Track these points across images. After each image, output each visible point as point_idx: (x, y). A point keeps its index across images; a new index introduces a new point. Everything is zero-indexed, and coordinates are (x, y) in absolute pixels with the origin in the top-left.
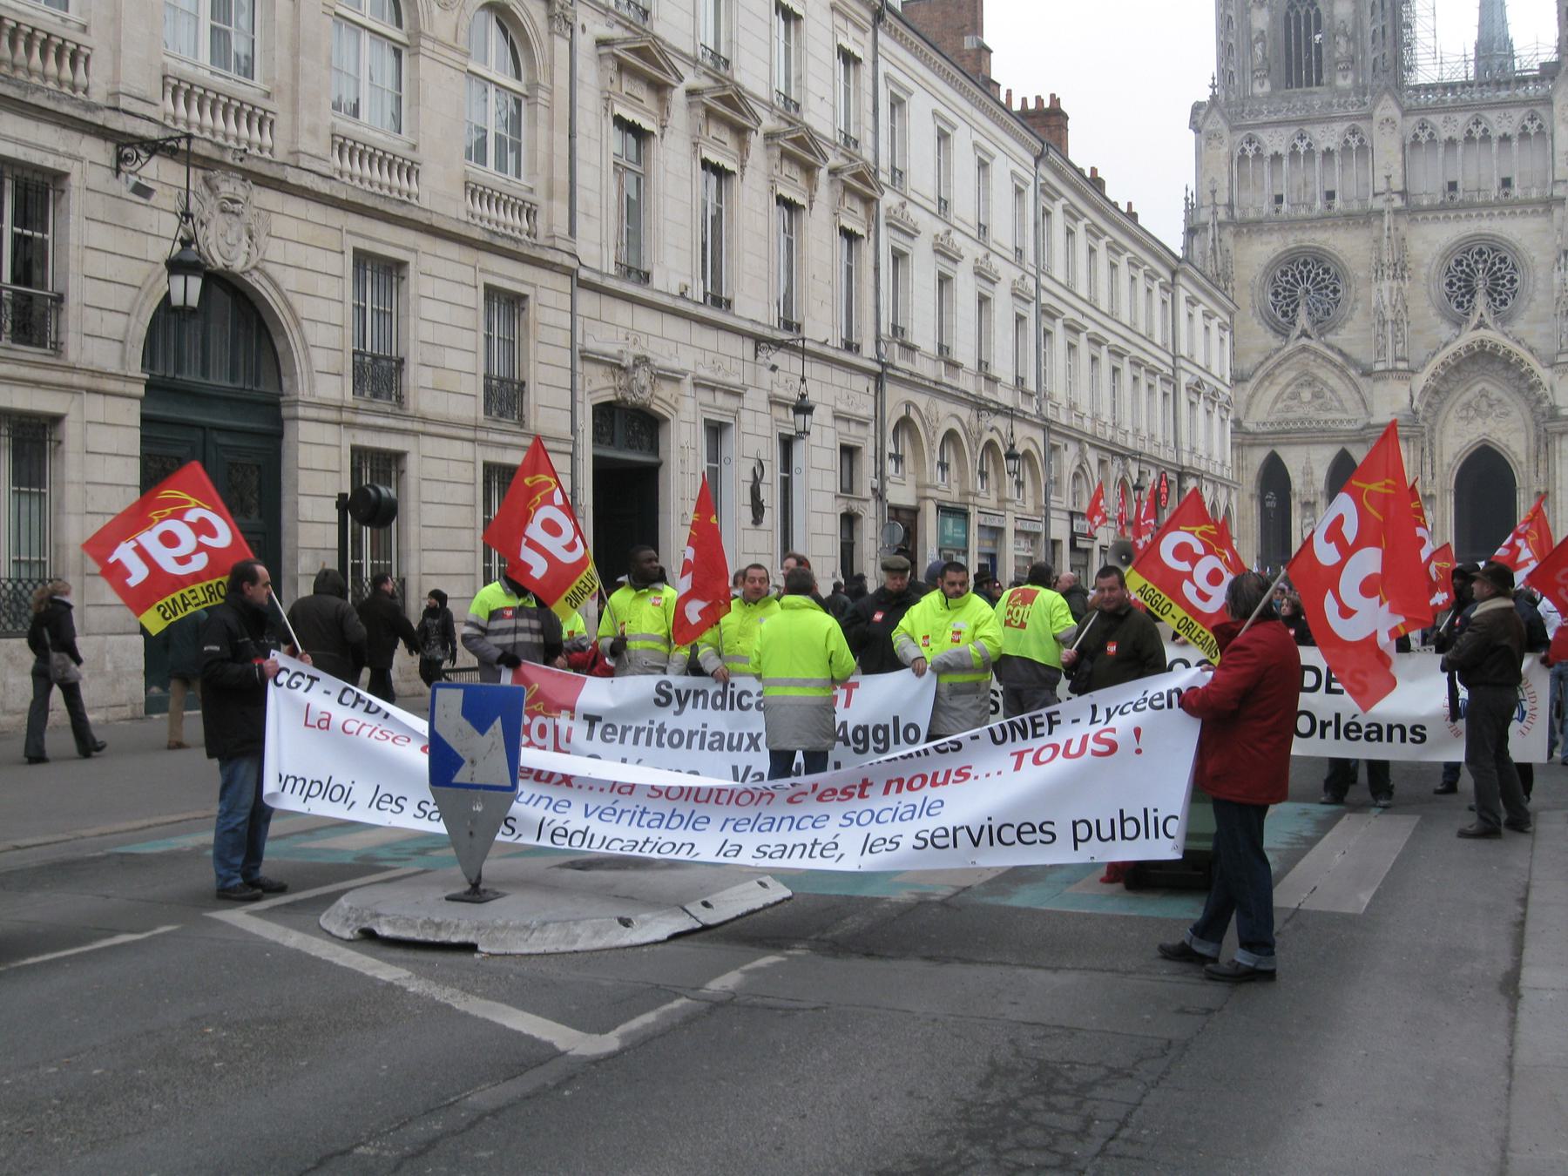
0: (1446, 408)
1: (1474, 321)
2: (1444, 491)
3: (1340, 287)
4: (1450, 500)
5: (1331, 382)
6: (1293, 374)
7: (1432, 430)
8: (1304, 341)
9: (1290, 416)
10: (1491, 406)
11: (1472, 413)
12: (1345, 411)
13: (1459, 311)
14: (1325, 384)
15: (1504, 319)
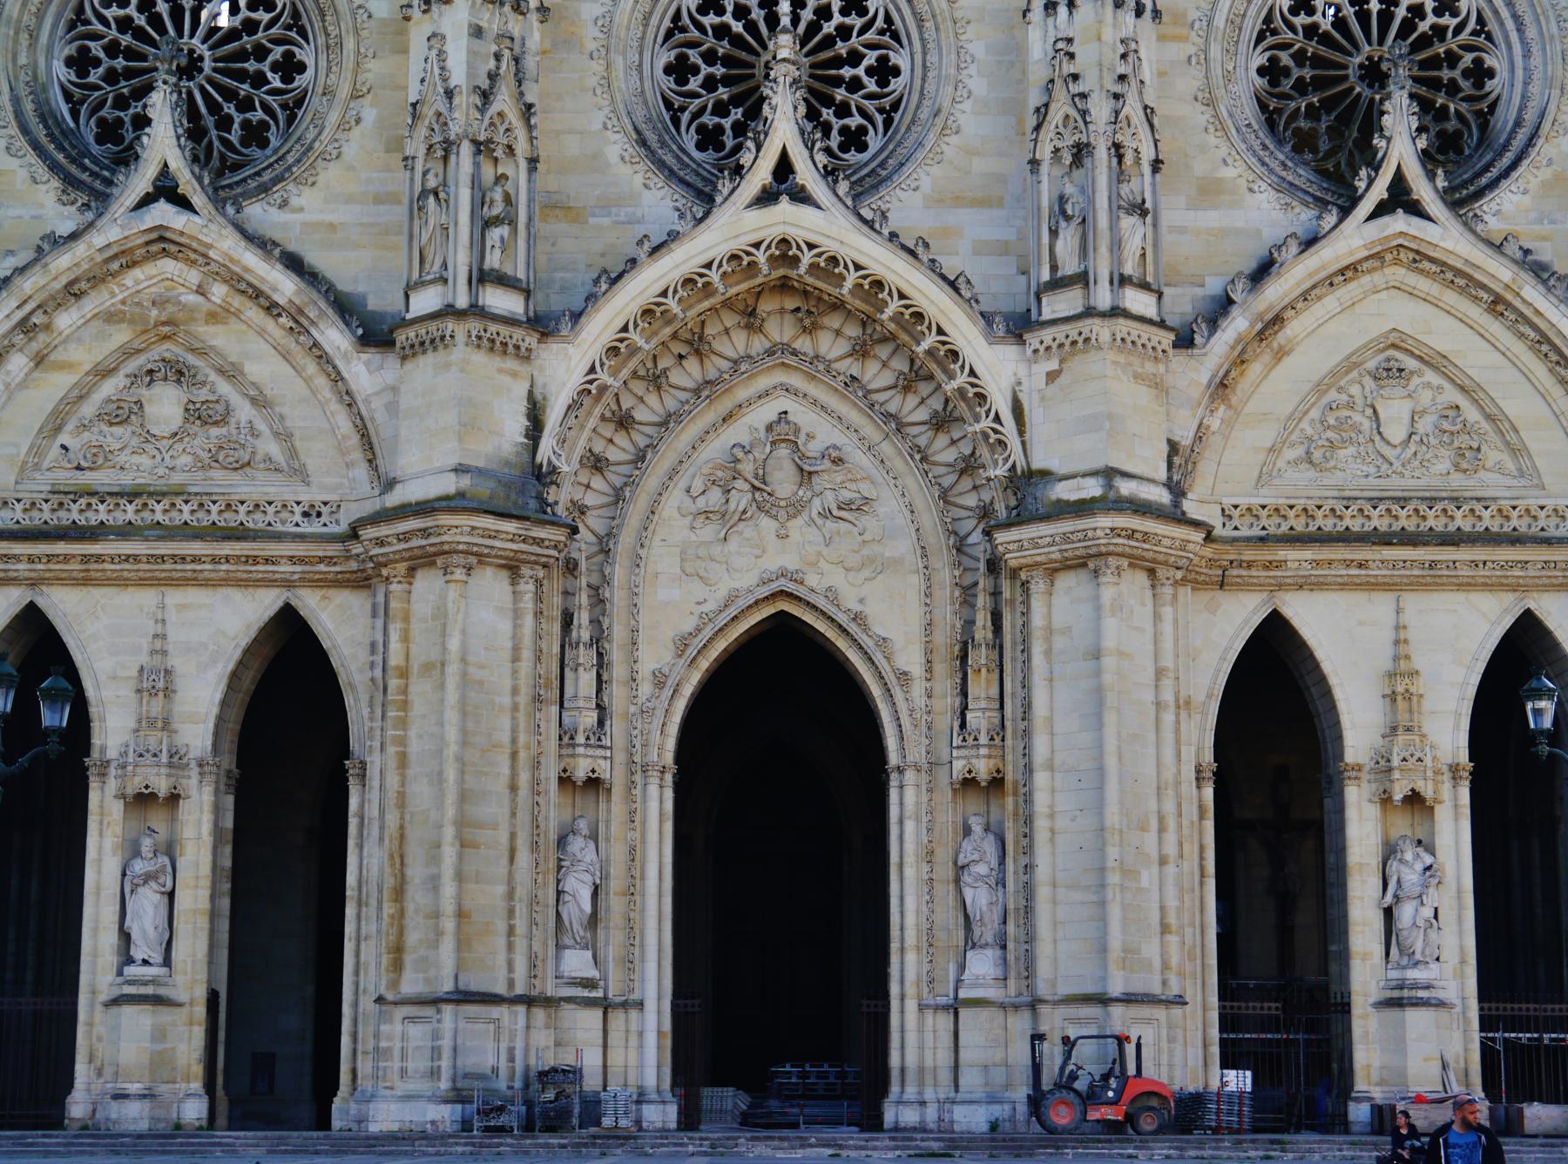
0: (651, 482)
1: (761, 174)
2: (637, 768)
3: (305, 54)
4: (659, 802)
5: (253, 370)
6: (121, 336)
7: (604, 548)
8: (162, 212)
9: (101, 479)
10: (806, 476)
11: (741, 499)
12: (300, 473)
13: (708, 156)
14: (231, 373)
15: (863, 187)
